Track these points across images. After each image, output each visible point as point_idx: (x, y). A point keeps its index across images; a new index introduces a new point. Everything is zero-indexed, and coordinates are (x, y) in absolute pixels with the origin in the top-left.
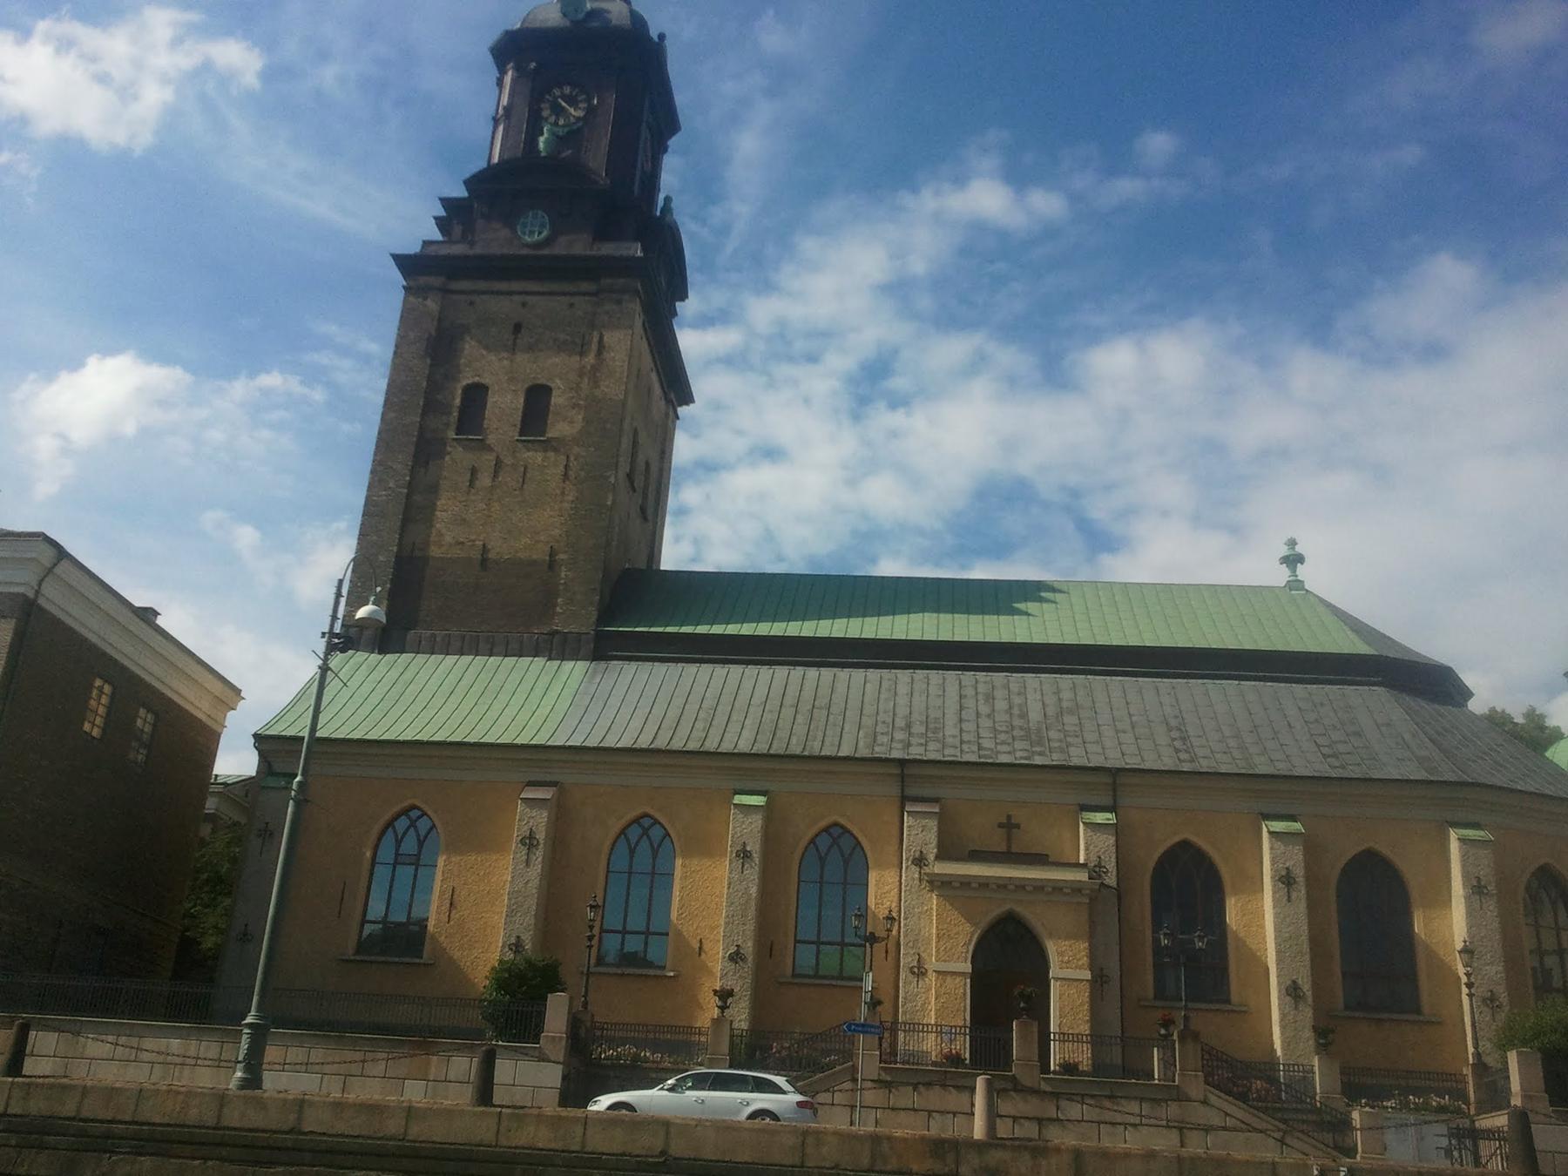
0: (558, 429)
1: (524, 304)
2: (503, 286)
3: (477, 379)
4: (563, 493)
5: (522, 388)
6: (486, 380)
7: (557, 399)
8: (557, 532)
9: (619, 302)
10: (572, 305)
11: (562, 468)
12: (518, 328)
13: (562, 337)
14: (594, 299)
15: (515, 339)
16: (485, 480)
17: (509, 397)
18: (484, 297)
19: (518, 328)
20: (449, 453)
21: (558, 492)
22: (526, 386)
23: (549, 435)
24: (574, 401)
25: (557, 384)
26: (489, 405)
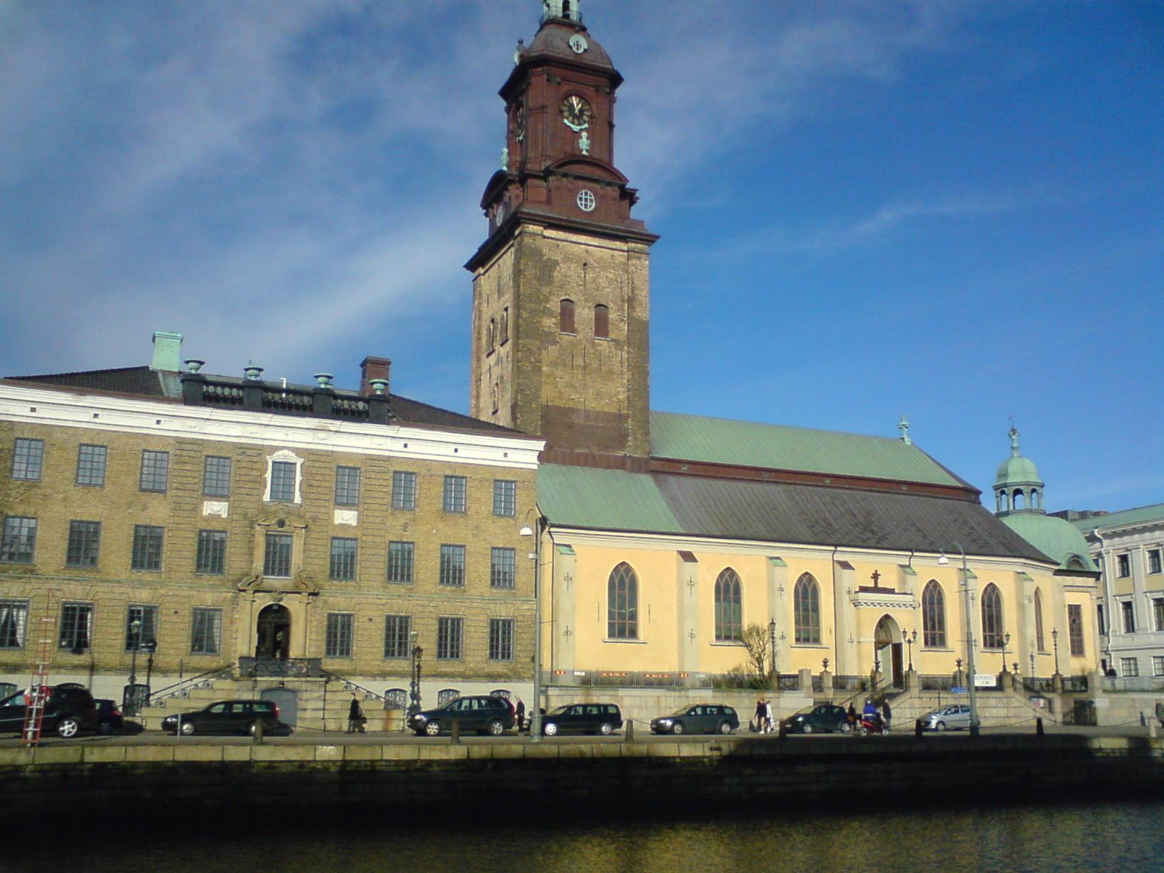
6: (572, 299)
17: (587, 310)
26: (576, 315)
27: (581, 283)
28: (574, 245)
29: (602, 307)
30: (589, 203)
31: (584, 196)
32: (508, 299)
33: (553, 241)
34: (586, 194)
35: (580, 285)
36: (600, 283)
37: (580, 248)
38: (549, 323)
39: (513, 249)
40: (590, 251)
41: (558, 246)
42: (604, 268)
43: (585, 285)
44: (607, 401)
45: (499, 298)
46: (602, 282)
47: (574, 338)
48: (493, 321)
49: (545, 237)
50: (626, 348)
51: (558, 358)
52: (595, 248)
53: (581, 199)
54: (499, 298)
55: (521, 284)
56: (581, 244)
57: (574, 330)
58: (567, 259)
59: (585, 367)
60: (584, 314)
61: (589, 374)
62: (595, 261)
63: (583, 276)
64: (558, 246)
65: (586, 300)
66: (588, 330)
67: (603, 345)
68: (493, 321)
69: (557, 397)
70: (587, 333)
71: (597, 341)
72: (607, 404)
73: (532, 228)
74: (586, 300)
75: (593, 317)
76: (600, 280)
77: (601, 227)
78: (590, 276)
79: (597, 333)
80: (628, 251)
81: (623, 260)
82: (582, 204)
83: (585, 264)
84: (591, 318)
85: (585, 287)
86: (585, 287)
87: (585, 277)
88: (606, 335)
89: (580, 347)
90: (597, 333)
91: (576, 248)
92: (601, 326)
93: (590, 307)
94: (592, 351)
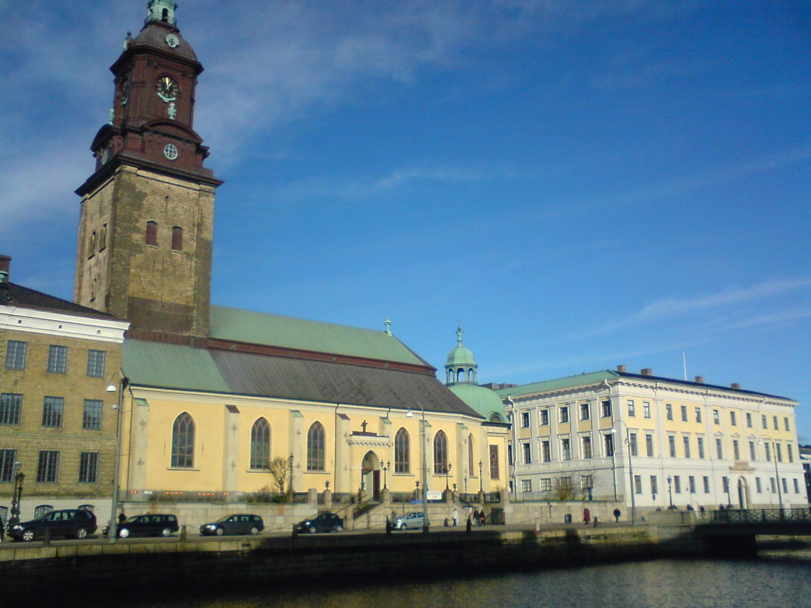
5: (171, 226)
6: (156, 221)
15: (167, 204)
26: (158, 233)
29: (179, 229)
30: (173, 154)
31: (169, 149)
32: (107, 217)
33: (144, 179)
35: (162, 212)
38: (138, 238)
39: (113, 182)
40: (171, 188)
43: (166, 211)
44: (179, 296)
45: (101, 217)
47: (156, 250)
48: (94, 233)
49: (138, 175)
50: (194, 259)
51: (144, 263)
53: (167, 151)
54: (101, 217)
55: (118, 207)
56: (165, 182)
57: (156, 244)
59: (163, 271)
60: (164, 233)
62: (175, 195)
63: (165, 205)
64: (148, 183)
66: (166, 244)
67: (178, 256)
68: (94, 233)
69: (141, 291)
71: (173, 253)
72: (178, 298)
73: (129, 168)
74: (167, 223)
75: (171, 235)
77: (181, 172)
78: (170, 206)
79: (173, 247)
80: (199, 190)
81: (196, 196)
82: (167, 154)
83: (167, 197)
84: (170, 236)
85: (166, 214)
86: (166, 214)
87: (166, 206)
90: (173, 247)
91: (161, 185)
92: (177, 242)
93: (169, 228)
94: (168, 259)
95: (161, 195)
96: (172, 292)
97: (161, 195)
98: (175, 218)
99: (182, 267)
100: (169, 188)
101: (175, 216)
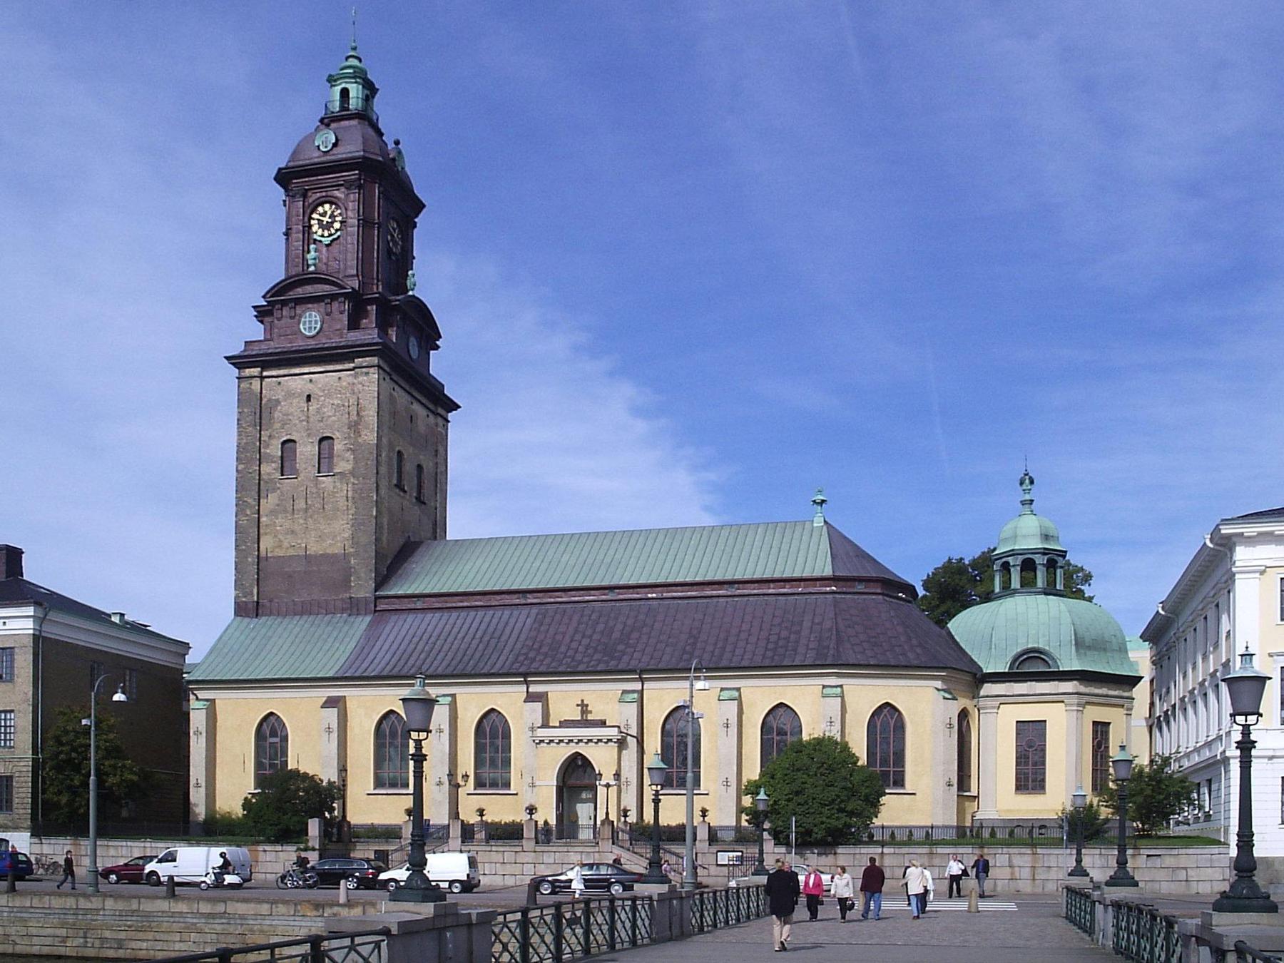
0: (342, 466)
1: (311, 381)
2: (297, 371)
3: (288, 437)
4: (348, 509)
7: (338, 446)
8: (346, 535)
9: (367, 373)
10: (340, 378)
11: (345, 492)
12: (309, 397)
13: (335, 402)
14: (352, 372)
16: (301, 504)
17: (309, 447)
18: (287, 378)
19: (309, 397)
20: (279, 488)
21: (345, 508)
22: (318, 438)
23: (335, 471)
24: (348, 446)
25: (337, 435)
27: (304, 418)
28: (296, 377)
30: (313, 325)
34: (310, 315)
35: (303, 421)
36: (324, 413)
37: (303, 379)
40: (314, 380)
41: (279, 383)
42: (329, 396)
43: (308, 417)
46: (328, 411)
52: (321, 375)
58: (290, 395)
60: (307, 451)
61: (311, 517)
63: (306, 409)
65: (309, 435)
70: (310, 472)
72: (331, 545)
74: (309, 435)
76: (325, 410)
78: (314, 406)
82: (305, 329)
84: (314, 455)
85: (308, 422)
88: (330, 469)
89: (302, 489)
95: (300, 395)
96: (321, 538)
97: (300, 395)
98: (322, 424)
99: (334, 497)
100: (311, 381)
101: (322, 421)
